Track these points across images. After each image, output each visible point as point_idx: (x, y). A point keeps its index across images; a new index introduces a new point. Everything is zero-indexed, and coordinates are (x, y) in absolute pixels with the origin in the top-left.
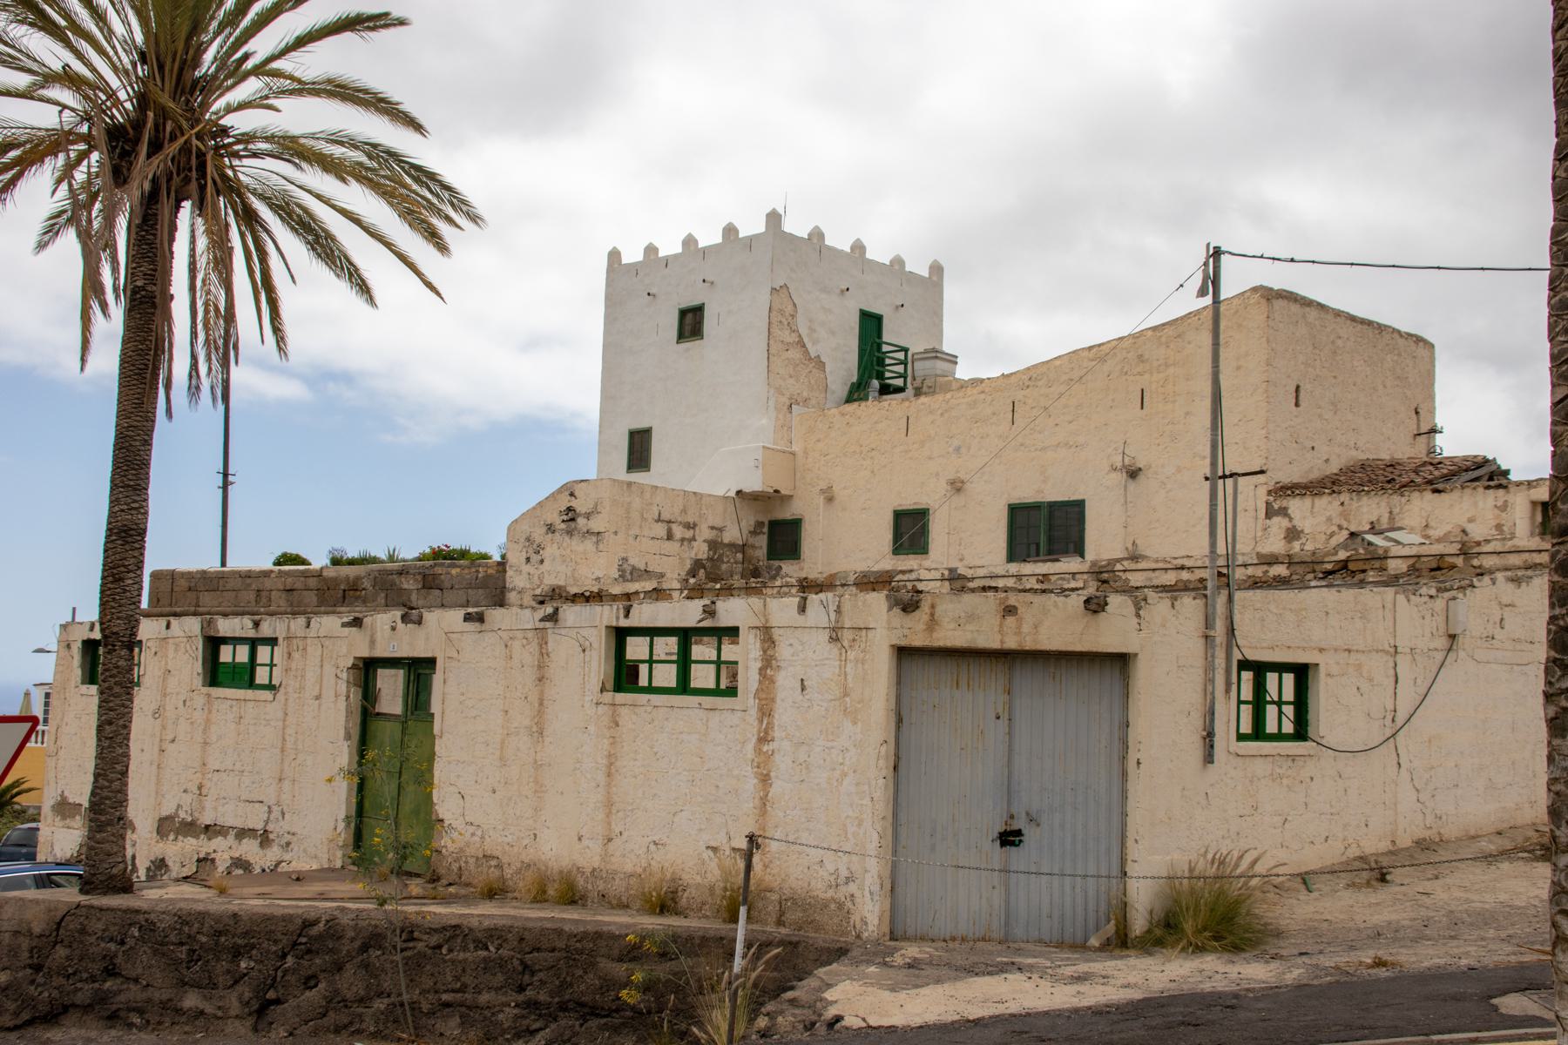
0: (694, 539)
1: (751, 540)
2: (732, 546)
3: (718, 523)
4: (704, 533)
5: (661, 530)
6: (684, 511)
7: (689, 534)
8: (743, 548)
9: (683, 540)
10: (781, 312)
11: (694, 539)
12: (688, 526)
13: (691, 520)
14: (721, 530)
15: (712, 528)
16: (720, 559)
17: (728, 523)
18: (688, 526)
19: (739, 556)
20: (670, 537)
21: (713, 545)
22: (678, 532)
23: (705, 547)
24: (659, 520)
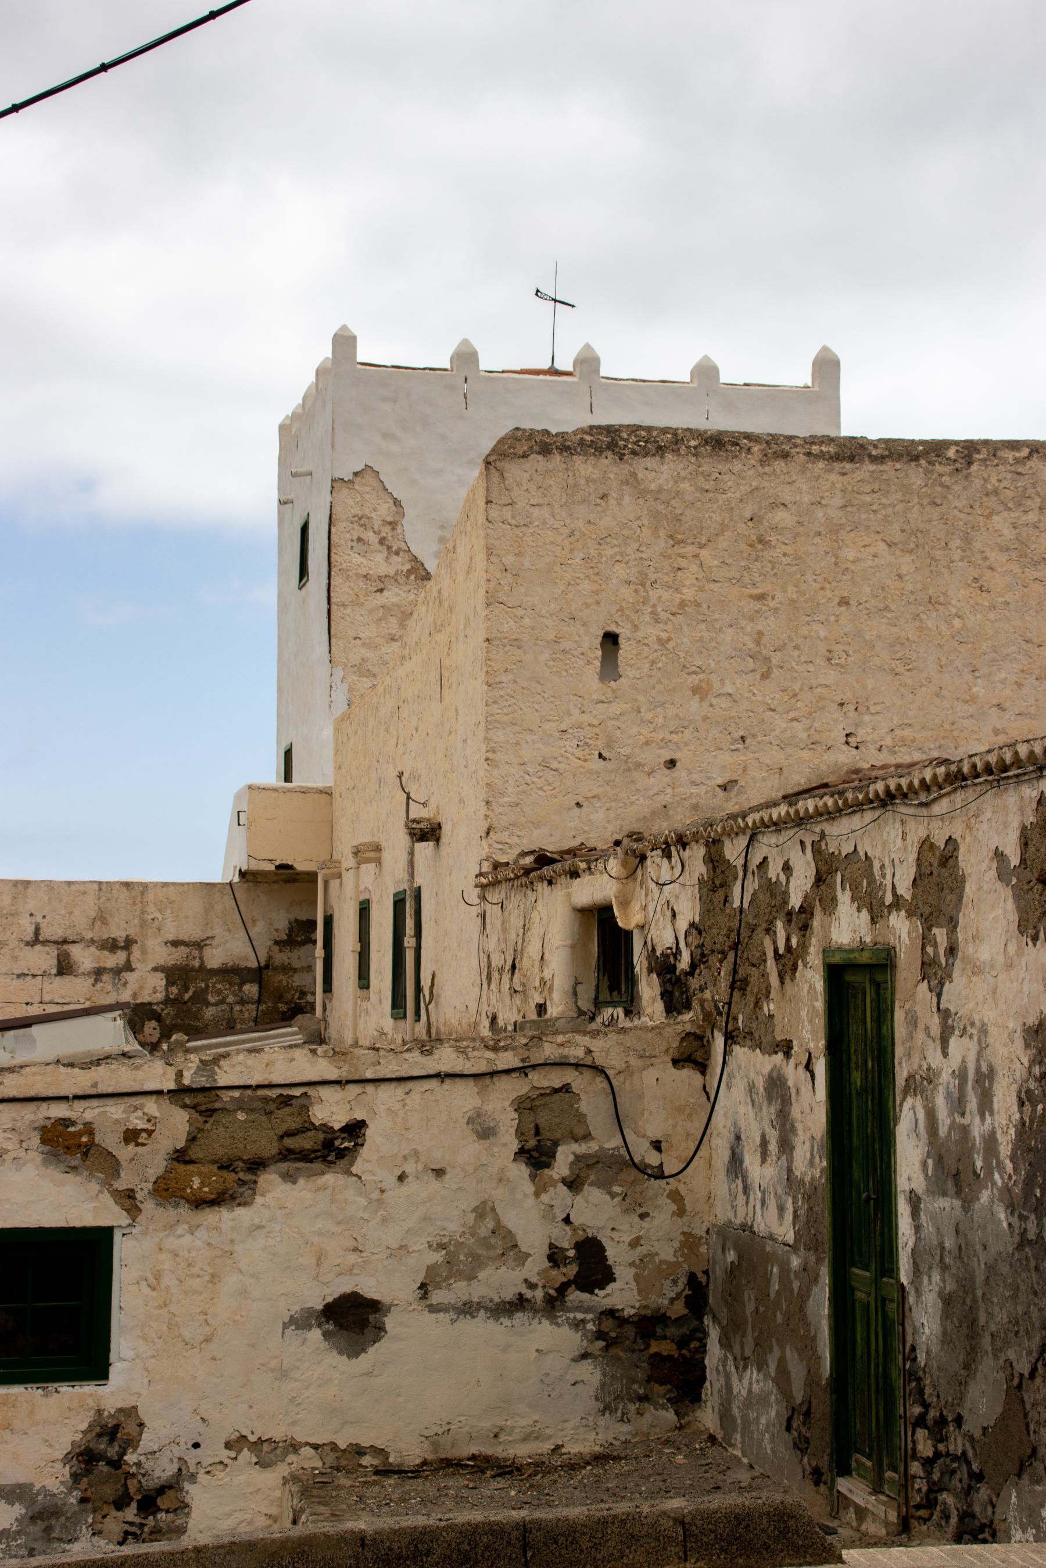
0: (128, 967)
1: (280, 957)
2: (232, 973)
3: (191, 931)
4: (155, 952)
5: (44, 959)
6: (102, 918)
7: (121, 957)
8: (259, 974)
9: (98, 973)
10: (362, 521)
11: (128, 967)
12: (111, 946)
13: (118, 932)
14: (199, 945)
15: (176, 943)
16: (200, 998)
17: (218, 931)
18: (111, 946)
19: (251, 989)
20: (65, 967)
21: (176, 975)
22: (85, 958)
23: (159, 981)
24: (36, 940)
